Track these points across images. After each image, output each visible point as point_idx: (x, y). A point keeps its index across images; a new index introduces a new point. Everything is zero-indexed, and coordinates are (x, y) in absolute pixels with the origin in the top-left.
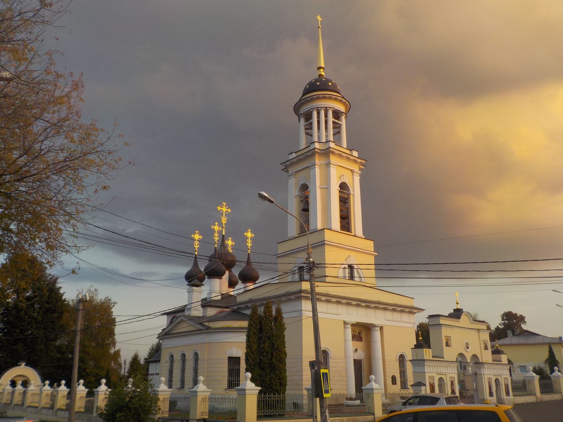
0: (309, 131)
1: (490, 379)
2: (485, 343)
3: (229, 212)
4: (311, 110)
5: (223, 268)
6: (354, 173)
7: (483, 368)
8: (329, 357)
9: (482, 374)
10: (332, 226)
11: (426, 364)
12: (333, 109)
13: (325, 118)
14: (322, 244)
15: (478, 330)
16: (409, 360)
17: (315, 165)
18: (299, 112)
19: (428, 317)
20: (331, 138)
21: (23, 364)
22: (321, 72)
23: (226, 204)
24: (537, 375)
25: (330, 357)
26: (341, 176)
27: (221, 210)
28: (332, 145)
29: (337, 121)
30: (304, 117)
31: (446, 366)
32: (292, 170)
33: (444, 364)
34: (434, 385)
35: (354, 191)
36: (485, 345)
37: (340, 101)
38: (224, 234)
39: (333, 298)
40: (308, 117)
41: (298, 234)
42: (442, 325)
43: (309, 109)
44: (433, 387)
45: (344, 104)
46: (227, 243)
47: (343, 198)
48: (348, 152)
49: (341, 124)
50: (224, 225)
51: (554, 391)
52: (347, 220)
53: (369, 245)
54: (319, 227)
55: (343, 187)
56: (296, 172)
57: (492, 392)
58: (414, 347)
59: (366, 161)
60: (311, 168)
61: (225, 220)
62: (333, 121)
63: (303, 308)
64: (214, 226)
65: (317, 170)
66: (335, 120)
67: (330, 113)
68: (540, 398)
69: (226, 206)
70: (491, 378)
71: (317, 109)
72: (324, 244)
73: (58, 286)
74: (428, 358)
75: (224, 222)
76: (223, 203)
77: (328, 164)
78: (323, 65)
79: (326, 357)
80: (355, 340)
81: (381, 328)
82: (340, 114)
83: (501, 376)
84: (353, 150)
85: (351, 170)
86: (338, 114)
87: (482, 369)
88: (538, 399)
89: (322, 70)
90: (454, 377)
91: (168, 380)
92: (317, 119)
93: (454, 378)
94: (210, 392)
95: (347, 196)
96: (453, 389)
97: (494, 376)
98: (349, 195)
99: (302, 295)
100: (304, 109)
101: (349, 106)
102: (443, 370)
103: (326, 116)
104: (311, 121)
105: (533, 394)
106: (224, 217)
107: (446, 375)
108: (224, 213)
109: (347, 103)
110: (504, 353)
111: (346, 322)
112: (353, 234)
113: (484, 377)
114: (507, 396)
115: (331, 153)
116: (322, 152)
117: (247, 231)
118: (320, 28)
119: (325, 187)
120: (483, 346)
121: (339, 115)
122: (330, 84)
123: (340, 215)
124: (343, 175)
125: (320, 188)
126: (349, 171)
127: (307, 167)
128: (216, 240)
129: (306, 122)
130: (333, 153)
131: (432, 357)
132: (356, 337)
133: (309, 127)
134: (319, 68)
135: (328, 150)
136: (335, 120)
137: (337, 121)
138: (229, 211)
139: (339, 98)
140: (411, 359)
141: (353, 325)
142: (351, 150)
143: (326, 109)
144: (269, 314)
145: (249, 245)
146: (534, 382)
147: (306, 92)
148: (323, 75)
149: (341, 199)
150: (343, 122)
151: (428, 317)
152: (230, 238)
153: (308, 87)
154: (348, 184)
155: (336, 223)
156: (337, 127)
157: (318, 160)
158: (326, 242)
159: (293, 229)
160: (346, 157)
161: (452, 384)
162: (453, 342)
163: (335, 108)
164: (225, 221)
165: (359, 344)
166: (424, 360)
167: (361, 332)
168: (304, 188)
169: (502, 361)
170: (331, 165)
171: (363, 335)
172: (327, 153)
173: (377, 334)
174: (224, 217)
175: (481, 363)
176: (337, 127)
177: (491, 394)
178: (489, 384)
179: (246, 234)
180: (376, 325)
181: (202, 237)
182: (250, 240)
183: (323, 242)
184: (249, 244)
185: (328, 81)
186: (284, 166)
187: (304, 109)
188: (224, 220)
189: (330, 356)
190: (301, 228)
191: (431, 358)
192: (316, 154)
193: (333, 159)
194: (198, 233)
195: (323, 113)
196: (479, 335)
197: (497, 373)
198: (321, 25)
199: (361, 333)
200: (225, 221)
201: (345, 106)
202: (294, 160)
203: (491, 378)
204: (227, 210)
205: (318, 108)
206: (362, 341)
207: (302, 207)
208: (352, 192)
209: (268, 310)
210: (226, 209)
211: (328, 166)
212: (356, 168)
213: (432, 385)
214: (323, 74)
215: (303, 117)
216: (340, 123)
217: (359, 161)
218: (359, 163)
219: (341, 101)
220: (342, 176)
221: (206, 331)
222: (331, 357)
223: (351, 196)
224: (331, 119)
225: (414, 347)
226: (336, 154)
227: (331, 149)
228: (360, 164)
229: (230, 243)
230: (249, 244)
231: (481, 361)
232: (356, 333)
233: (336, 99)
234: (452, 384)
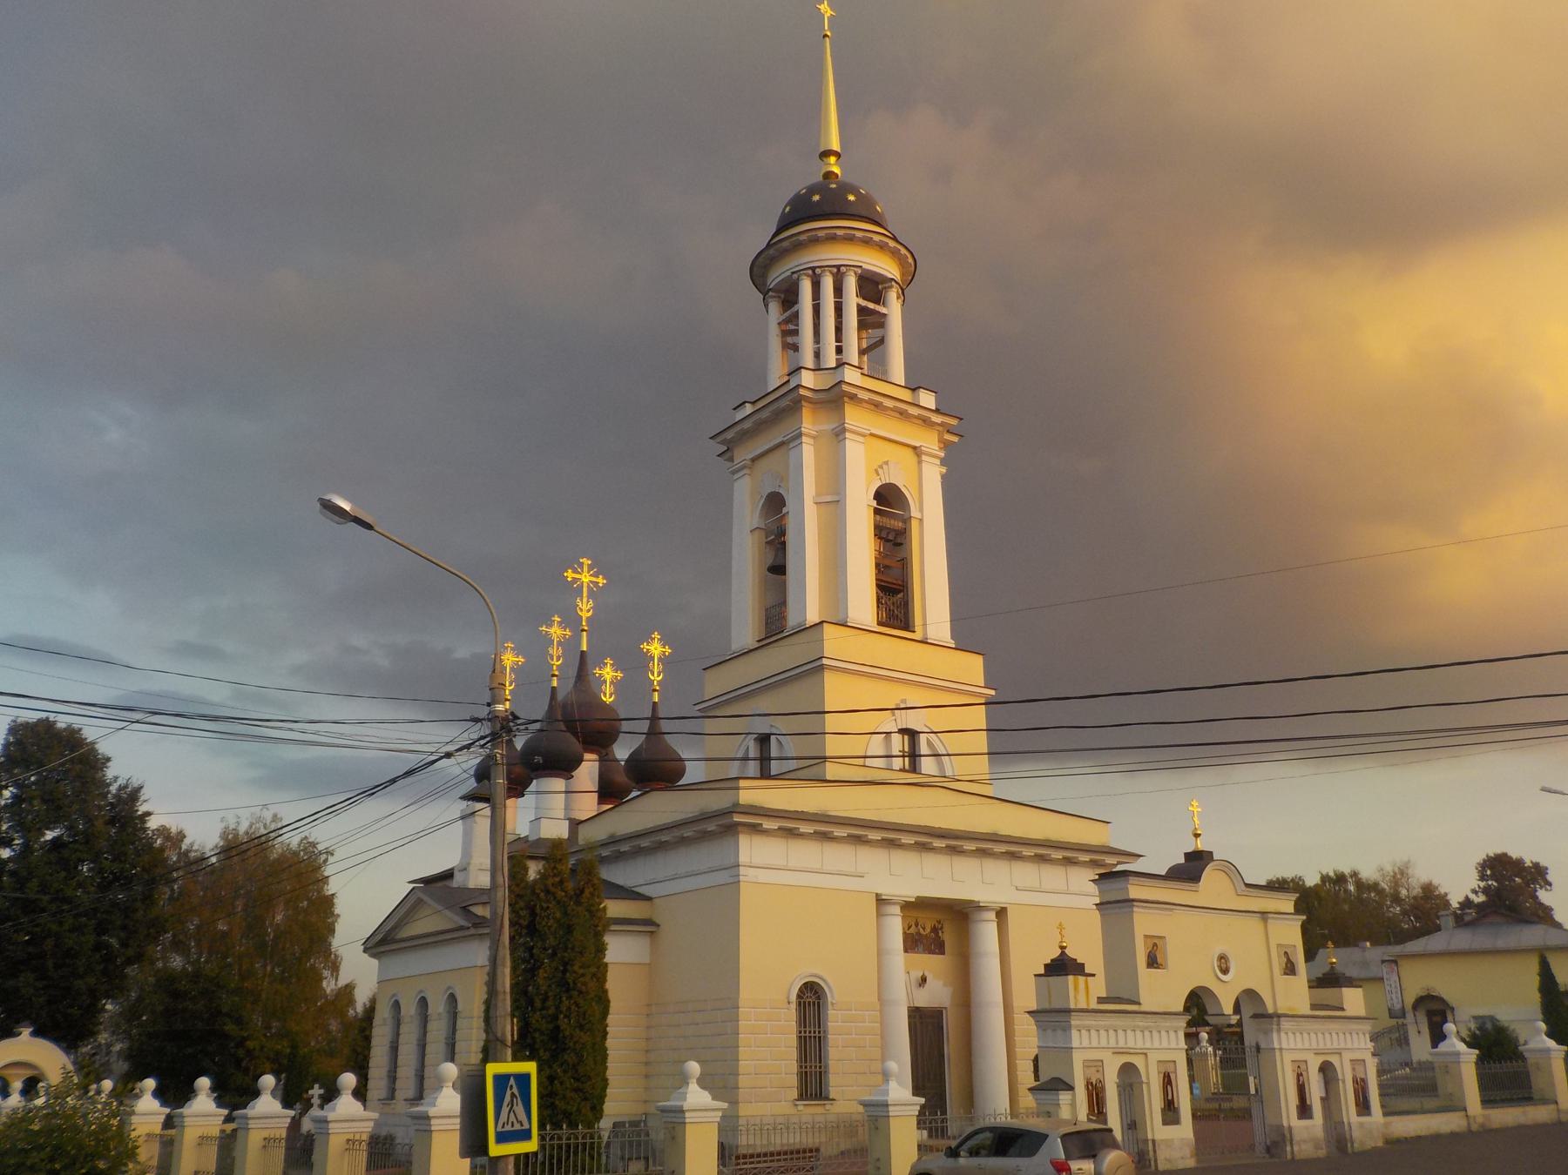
0: (790, 340)
1: (1303, 1067)
2: (1286, 953)
3: (601, 585)
4: (795, 276)
5: (574, 744)
6: (924, 458)
7: (1279, 1031)
8: (826, 1002)
9: (1274, 1049)
10: (849, 615)
11: (1073, 1023)
12: (859, 271)
13: (835, 298)
14: (815, 668)
15: (1264, 915)
16: (1029, 1012)
17: (800, 435)
18: (764, 284)
19: (1097, 877)
20: (852, 355)
21: (26, 1032)
22: (830, 164)
23: (590, 562)
24: (1562, 1045)
25: (829, 1003)
26: (881, 467)
27: (575, 580)
28: (851, 376)
29: (871, 306)
30: (779, 297)
31: (1147, 1028)
32: (743, 454)
33: (1140, 1022)
34: (1103, 1088)
35: (921, 510)
36: (1289, 960)
37: (881, 248)
38: (585, 649)
39: (840, 826)
40: (789, 297)
41: (758, 641)
42: (1135, 903)
43: (788, 273)
44: (1097, 1095)
45: (894, 253)
46: (601, 675)
47: (890, 530)
48: (906, 395)
49: (885, 315)
50: (584, 623)
51: (1535, 1097)
52: (901, 595)
53: (971, 668)
54: (812, 616)
55: (888, 498)
56: (753, 460)
57: (1308, 1103)
58: (1043, 972)
59: (961, 419)
60: (791, 445)
61: (589, 606)
62: (858, 305)
63: (743, 859)
64: (550, 625)
65: (808, 451)
66: (864, 303)
67: (851, 283)
68: (1480, 1120)
69: (590, 568)
70: (1306, 1062)
71: (810, 272)
72: (822, 668)
73: (142, 809)
74: (1083, 1005)
75: (585, 615)
76: (581, 560)
77: (840, 433)
78: (836, 146)
79: (819, 1003)
80: (921, 949)
81: (1001, 913)
82: (882, 284)
83: (1340, 1054)
84: (920, 387)
85: (915, 448)
86: (877, 284)
87: (1275, 1035)
88: (1472, 1121)
89: (833, 159)
90: (1175, 1062)
91: (416, 1075)
92: (813, 301)
93: (1172, 1064)
94: (371, 1120)
95: (900, 524)
96: (1170, 1097)
97: (1315, 1054)
98: (907, 520)
99: (735, 819)
100: (777, 275)
101: (910, 260)
102: (1135, 1040)
103: (839, 291)
104: (795, 309)
105: (1454, 1105)
106: (585, 600)
107: (1146, 1054)
108: (585, 589)
109: (903, 251)
111: (884, 897)
112: (918, 636)
113: (1282, 1059)
114: (1359, 1114)
115: (846, 399)
116: (820, 396)
117: (649, 640)
118: (827, 39)
119: (829, 499)
120: (1278, 964)
121: (880, 287)
122: (851, 198)
123: (876, 580)
124: (886, 463)
125: (816, 503)
126: (909, 453)
127: (782, 444)
128: (555, 668)
129: (785, 311)
130: (853, 397)
131: (1098, 1003)
132: (925, 941)
133: (790, 330)
134: (826, 154)
135: (837, 388)
136: (864, 303)
137: (871, 306)
138: (601, 581)
139: (877, 238)
140: (1034, 1006)
141: (907, 906)
142: (914, 390)
143: (839, 270)
144: (557, 879)
145: (656, 678)
146: (1460, 1074)
147: (786, 223)
148: (837, 175)
149: (884, 535)
150: (893, 308)
151: (1097, 877)
152: (609, 661)
154: (903, 490)
155: (862, 601)
156: (871, 321)
157: (809, 422)
158: (825, 661)
159: (745, 631)
160: (895, 410)
161: (1167, 1081)
162: (1173, 954)
163: (865, 266)
164: (588, 611)
165: (929, 963)
166: (1068, 1011)
167: (940, 926)
168: (775, 504)
169: (1345, 1007)
170: (848, 435)
171: (948, 937)
172: (835, 398)
173: (987, 933)
174: (585, 600)
175: (1270, 1016)
176: (871, 321)
177: (1304, 1110)
178: (1299, 1081)
179: (645, 646)
180: (981, 904)
181: (522, 660)
182: (658, 665)
183: (818, 663)
184: (656, 675)
185: (846, 188)
186: (722, 443)
187: (777, 275)
188: (585, 608)
189: (829, 999)
190: (767, 624)
191: (1094, 1005)
192: (804, 403)
193: (854, 417)
194: (512, 649)
195: (828, 283)
196: (1266, 927)
197: (1329, 1045)
198: (830, 29)
199: (942, 928)
200: (588, 611)
201: (900, 259)
202: (747, 425)
203: (1306, 1062)
204: (594, 579)
205: (813, 269)
206: (943, 953)
207: (770, 562)
208: (914, 513)
209: (555, 868)
210: (591, 575)
211: (841, 437)
212: (930, 442)
213: (1095, 1087)
214: (836, 170)
215: (777, 299)
216: (883, 310)
217: (937, 419)
218: (938, 424)
219: (882, 247)
220: (885, 467)
221: (472, 931)
222: (832, 1004)
223: (914, 524)
224: (852, 300)
225: (1043, 972)
226: (862, 401)
227: (845, 387)
228: (941, 429)
229: (608, 673)
230: (656, 675)
231: (1271, 1011)
232: (924, 929)
233: (867, 242)
234: (1167, 1081)
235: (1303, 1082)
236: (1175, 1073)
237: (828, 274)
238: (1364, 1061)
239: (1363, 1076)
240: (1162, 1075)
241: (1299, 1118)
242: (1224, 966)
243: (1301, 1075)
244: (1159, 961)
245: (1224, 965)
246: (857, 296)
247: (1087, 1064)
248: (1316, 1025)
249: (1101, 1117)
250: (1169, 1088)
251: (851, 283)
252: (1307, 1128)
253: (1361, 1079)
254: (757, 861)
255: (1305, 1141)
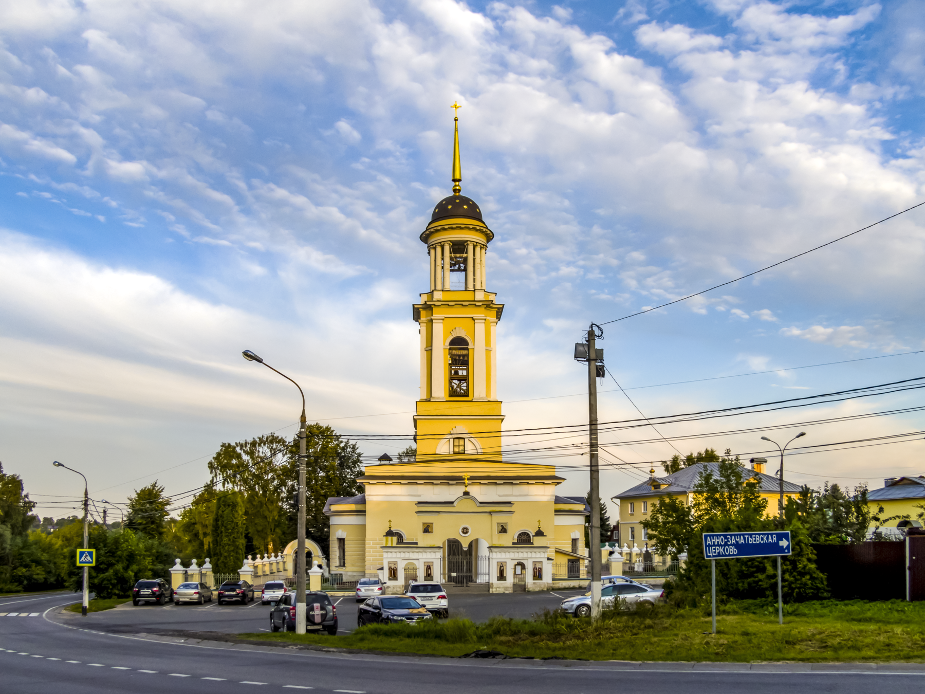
1: (504, 564)
2: (502, 526)
6: (476, 321)
15: (490, 512)
34: (397, 570)
55: (459, 343)
57: (505, 575)
70: (506, 562)
74: (389, 545)
85: (472, 318)
96: (429, 573)
110: (545, 534)
130: (434, 305)
153: (471, 203)
161: (429, 568)
170: (434, 321)
177: (502, 577)
203: (506, 562)
223: (471, 351)
234: (429, 568)
235: (503, 569)
236: (433, 565)
237: (446, 244)
238: (542, 562)
239: (540, 567)
240: (426, 567)
241: (498, 580)
242: (465, 531)
243: (503, 566)
244: (430, 530)
245: (465, 531)
246: (450, 253)
247: (389, 563)
248: (516, 550)
249: (395, 578)
250: (429, 570)
251: (447, 248)
252: (502, 584)
253: (539, 568)
254: (372, 493)
255: (499, 588)
